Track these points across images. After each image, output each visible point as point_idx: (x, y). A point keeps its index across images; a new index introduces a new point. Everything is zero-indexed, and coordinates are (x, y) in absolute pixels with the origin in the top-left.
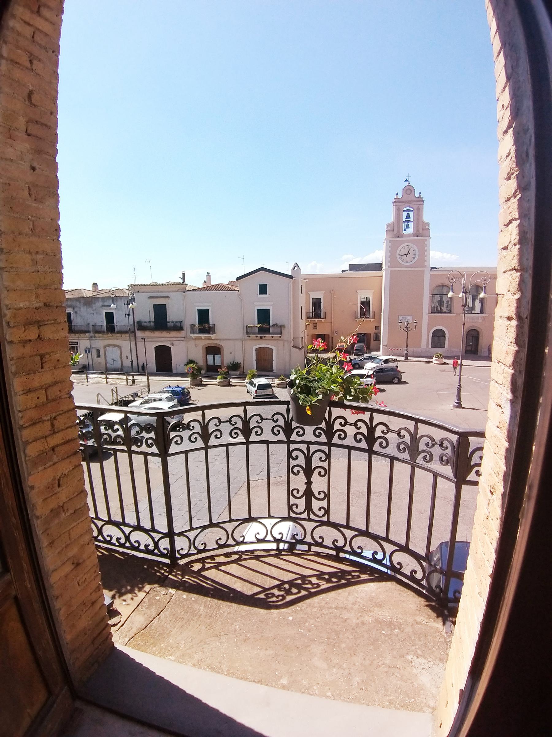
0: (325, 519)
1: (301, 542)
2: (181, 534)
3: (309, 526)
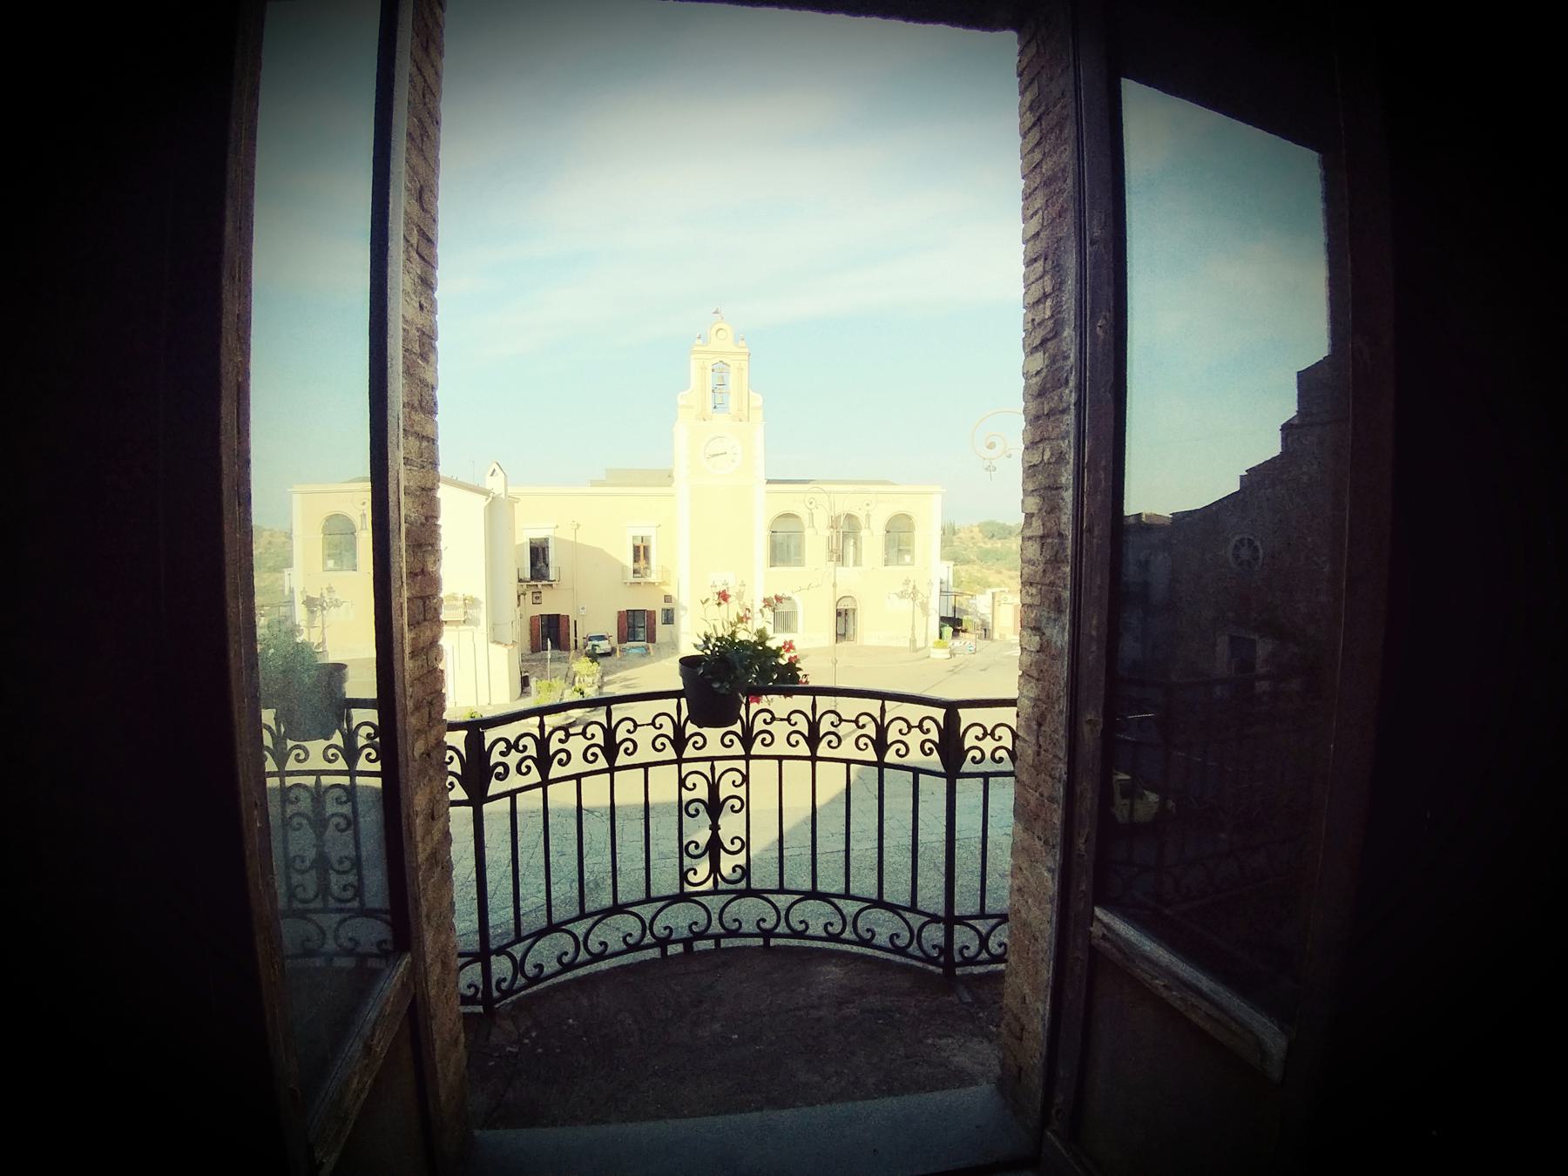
0: (742, 885)
2: (501, 951)
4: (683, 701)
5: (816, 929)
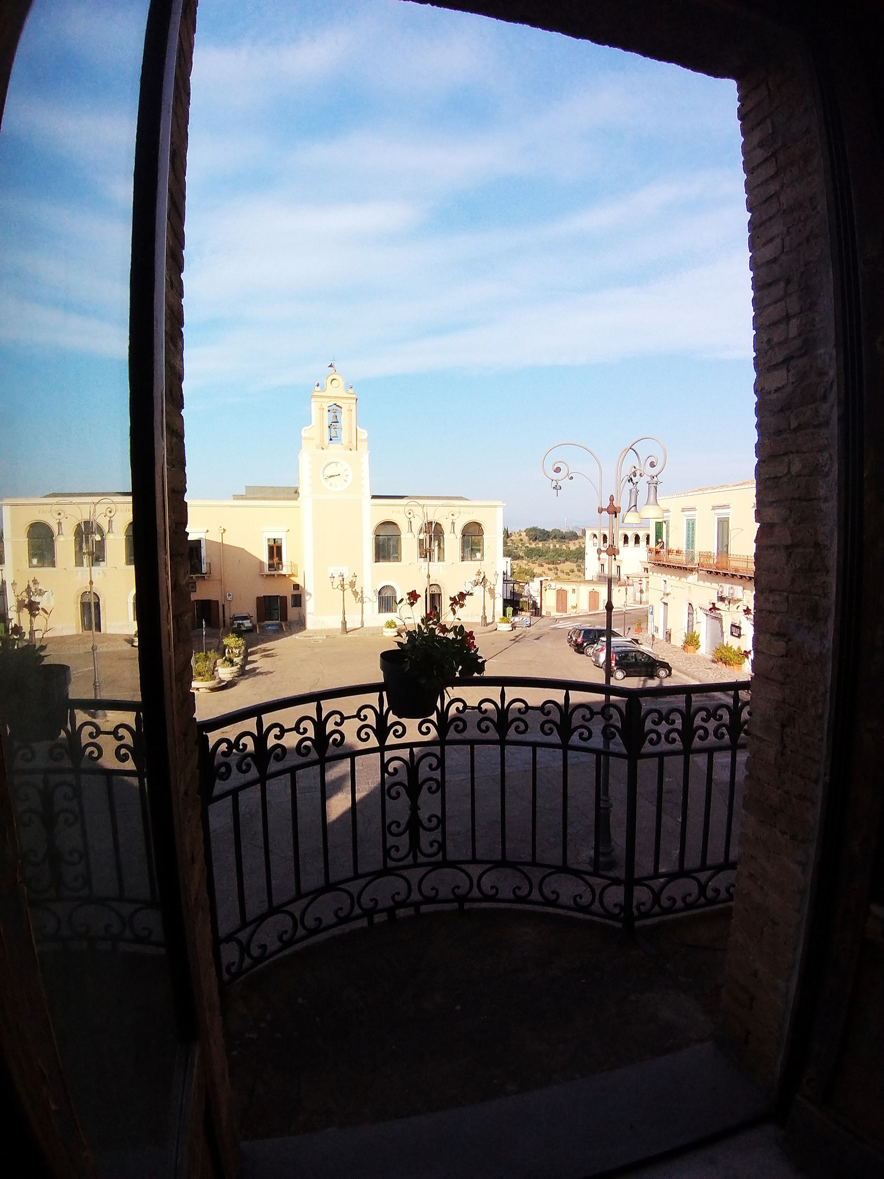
0: (439, 857)
1: (402, 904)
3: (414, 875)
4: (384, 693)
5: (506, 892)
